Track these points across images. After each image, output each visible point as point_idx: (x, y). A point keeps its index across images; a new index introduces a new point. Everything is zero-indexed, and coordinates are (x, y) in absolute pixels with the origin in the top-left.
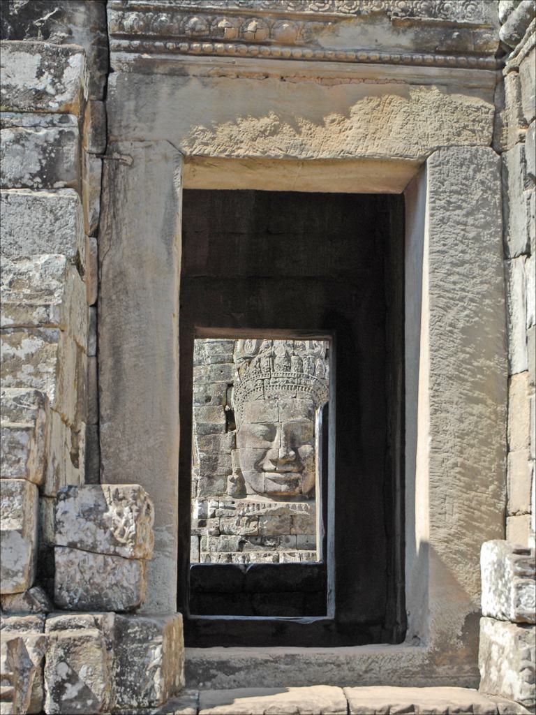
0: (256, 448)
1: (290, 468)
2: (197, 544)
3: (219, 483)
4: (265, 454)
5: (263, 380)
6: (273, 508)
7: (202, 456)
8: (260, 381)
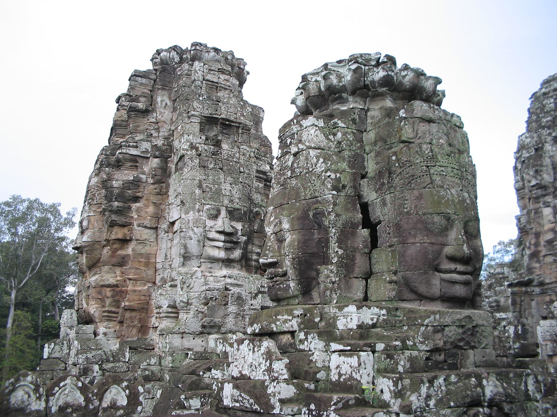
0: (433, 243)
3: (358, 286)
5: (428, 167)
6: (459, 316)
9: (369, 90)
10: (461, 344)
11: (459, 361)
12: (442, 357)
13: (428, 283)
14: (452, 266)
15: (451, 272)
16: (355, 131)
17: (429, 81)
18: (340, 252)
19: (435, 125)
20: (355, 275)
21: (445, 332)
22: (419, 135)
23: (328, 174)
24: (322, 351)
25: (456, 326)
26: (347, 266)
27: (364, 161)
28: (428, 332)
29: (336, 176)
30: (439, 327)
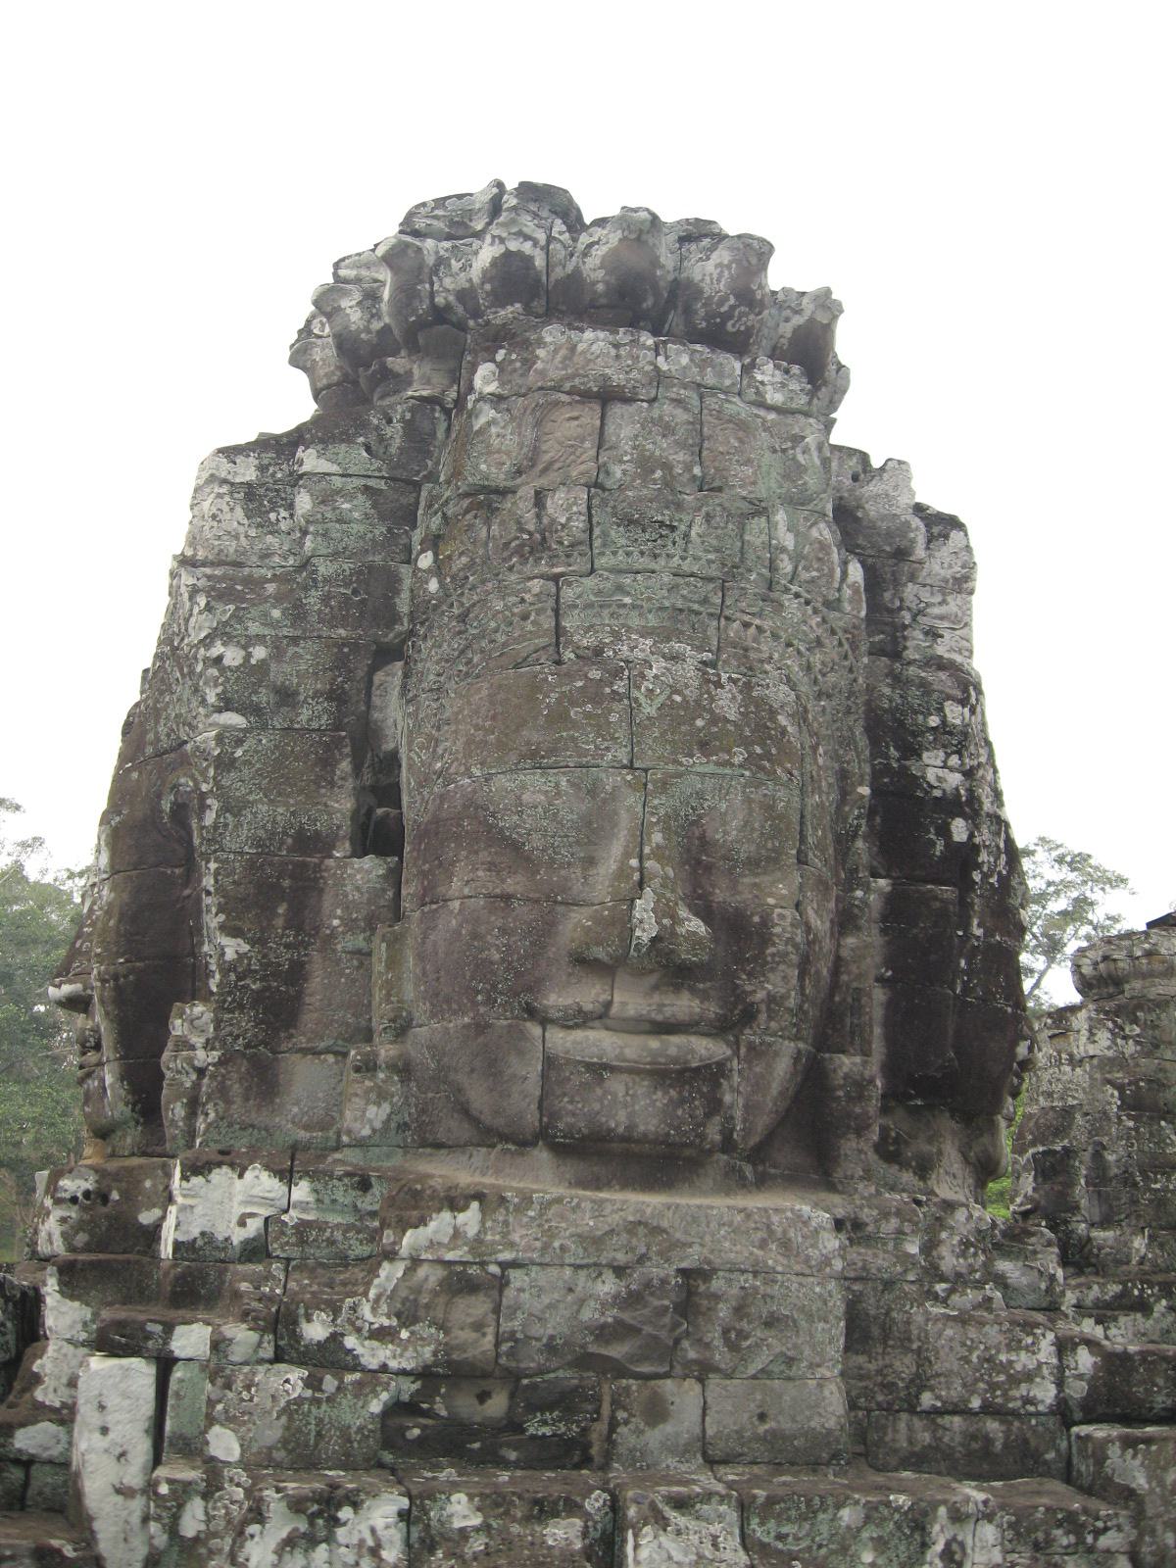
0: (507, 898)
1: (683, 1005)
2: (148, 1408)
4: (544, 931)
5: (555, 578)
7: (230, 955)
8: (536, 585)
9: (462, 327)
10: (617, 1351)
11: (601, 1427)
12: (497, 1405)
13: (492, 1068)
14: (588, 994)
15: (580, 1019)
16: (382, 485)
17: (715, 256)
18: (233, 947)
19: (632, 408)
20: (302, 1041)
21: (510, 1293)
22: (547, 457)
23: (218, 649)
24: (69, 1341)
25: (577, 1267)
26: (273, 1007)
27: (397, 592)
28: (418, 1290)
29: (249, 655)
30: (472, 1271)
